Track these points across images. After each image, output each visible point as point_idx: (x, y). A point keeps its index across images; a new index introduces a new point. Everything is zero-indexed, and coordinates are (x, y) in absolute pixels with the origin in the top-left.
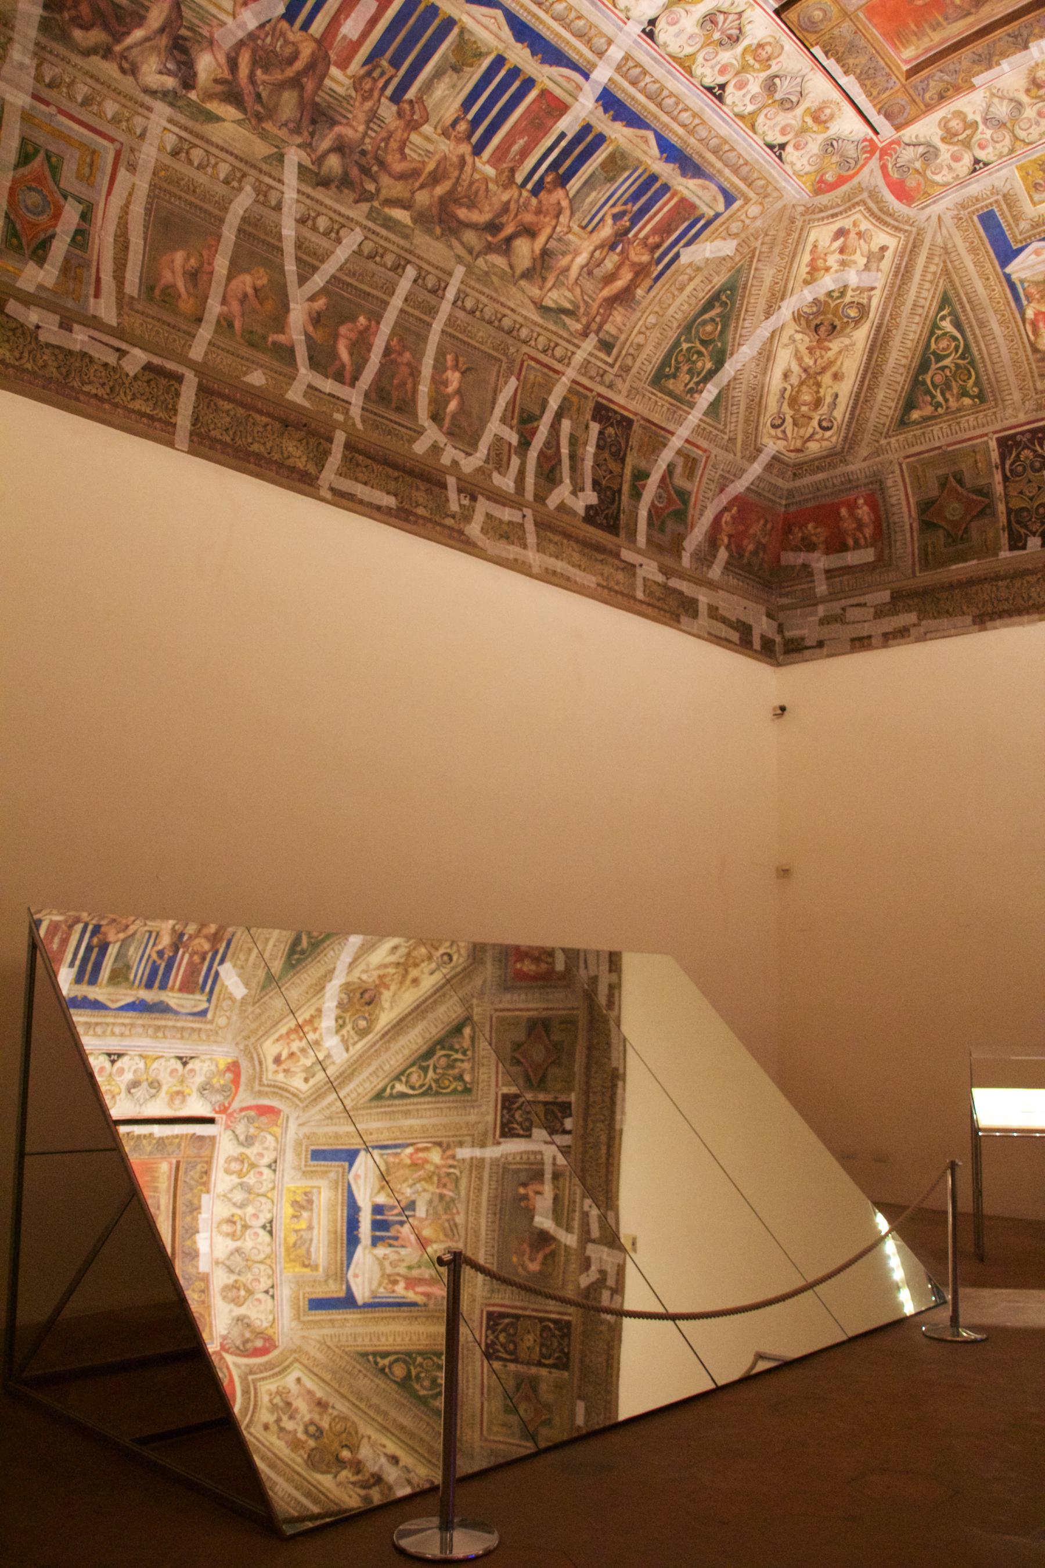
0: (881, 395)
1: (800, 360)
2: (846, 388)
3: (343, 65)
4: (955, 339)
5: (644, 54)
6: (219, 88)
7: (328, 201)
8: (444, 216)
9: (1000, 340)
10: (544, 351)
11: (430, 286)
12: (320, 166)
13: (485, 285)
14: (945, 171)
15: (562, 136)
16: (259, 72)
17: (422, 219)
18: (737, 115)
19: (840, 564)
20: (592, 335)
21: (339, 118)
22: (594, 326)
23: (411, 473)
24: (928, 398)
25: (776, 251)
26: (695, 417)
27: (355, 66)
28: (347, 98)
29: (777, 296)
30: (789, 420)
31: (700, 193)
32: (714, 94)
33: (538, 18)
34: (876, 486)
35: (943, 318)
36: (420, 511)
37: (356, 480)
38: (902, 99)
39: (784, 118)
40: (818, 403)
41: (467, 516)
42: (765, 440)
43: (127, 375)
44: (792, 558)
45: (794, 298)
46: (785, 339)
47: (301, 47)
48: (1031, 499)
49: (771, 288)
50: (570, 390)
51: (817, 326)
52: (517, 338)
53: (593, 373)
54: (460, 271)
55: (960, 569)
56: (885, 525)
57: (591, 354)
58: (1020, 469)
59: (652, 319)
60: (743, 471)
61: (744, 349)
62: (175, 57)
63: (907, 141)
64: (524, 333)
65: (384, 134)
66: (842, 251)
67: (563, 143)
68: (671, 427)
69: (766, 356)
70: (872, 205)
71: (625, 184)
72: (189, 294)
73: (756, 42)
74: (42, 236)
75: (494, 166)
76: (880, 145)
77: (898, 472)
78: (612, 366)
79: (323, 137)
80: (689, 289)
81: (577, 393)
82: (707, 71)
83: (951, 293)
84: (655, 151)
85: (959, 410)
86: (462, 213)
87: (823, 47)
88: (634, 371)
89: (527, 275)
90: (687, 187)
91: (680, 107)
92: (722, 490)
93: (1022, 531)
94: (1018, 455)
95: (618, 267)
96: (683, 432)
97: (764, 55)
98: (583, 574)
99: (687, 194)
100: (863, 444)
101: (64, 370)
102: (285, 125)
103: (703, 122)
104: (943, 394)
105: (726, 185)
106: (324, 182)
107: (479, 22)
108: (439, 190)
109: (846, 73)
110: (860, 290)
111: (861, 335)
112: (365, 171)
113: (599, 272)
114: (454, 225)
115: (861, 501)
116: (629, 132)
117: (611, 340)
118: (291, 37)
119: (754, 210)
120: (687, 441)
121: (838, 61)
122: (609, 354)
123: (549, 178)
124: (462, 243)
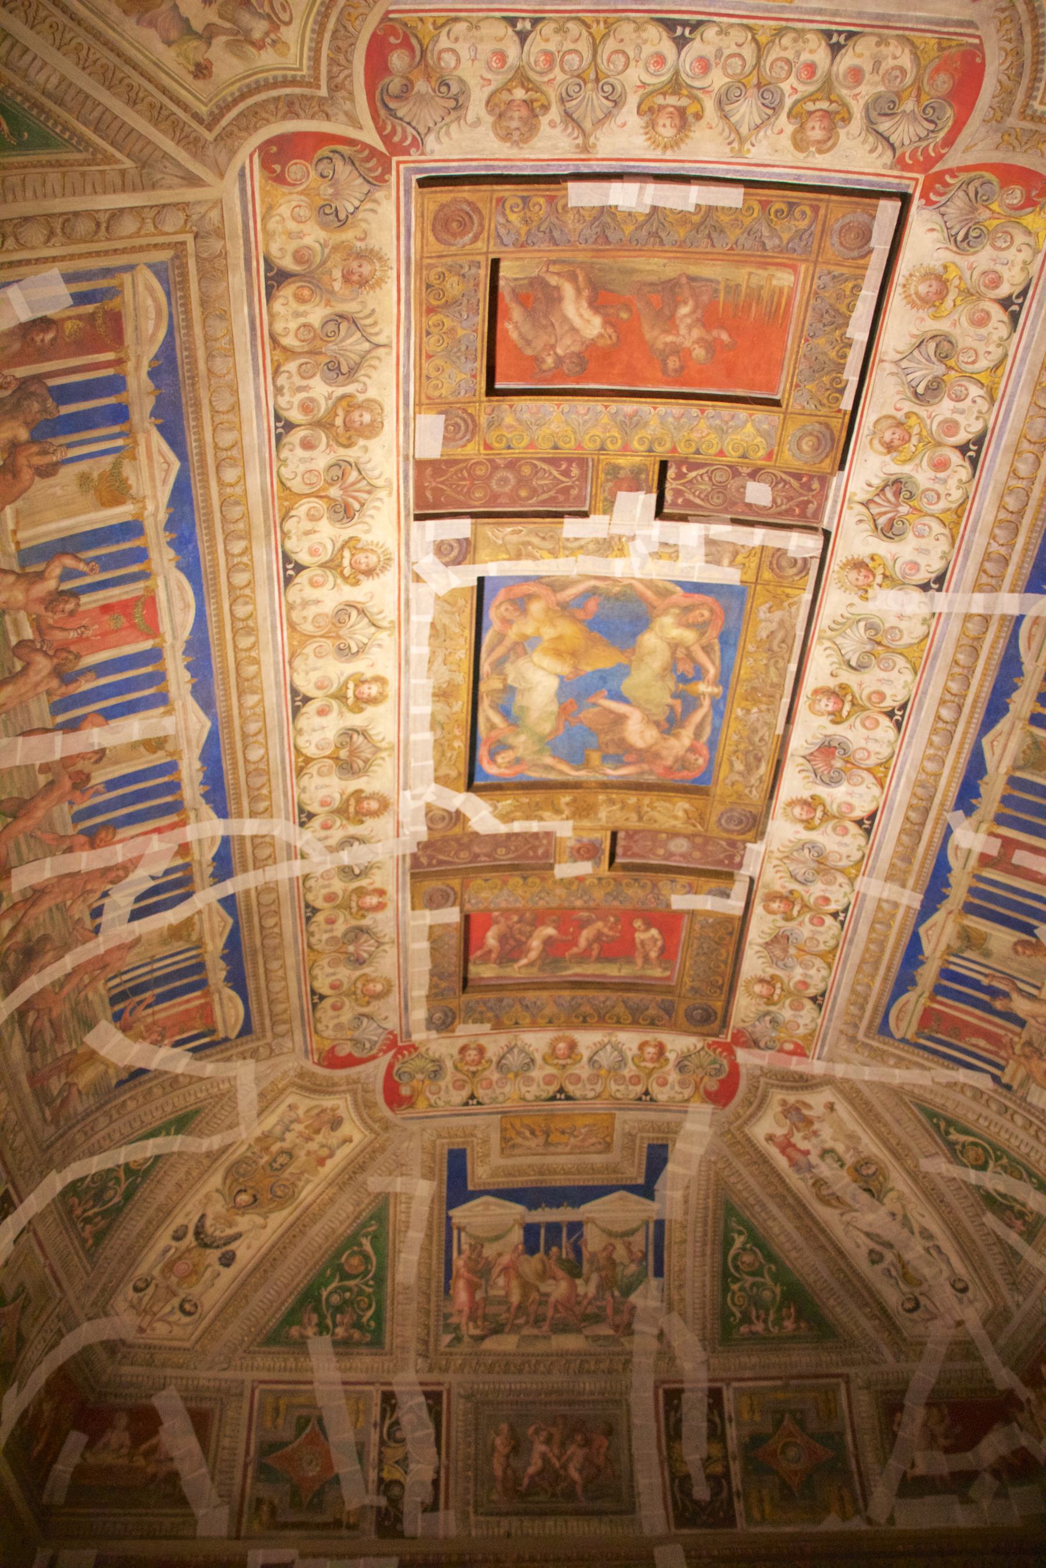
5: (967, 571)
18: (992, 401)
32: (978, 452)
33: (975, 701)
38: (833, 246)
39: (965, 335)
63: (889, 153)
73: (888, 458)
76: (921, 177)
82: (953, 483)
87: (837, 400)
91: (1013, 483)
97: (899, 433)
103: (1023, 436)
107: (1002, 755)
121: (841, 368)
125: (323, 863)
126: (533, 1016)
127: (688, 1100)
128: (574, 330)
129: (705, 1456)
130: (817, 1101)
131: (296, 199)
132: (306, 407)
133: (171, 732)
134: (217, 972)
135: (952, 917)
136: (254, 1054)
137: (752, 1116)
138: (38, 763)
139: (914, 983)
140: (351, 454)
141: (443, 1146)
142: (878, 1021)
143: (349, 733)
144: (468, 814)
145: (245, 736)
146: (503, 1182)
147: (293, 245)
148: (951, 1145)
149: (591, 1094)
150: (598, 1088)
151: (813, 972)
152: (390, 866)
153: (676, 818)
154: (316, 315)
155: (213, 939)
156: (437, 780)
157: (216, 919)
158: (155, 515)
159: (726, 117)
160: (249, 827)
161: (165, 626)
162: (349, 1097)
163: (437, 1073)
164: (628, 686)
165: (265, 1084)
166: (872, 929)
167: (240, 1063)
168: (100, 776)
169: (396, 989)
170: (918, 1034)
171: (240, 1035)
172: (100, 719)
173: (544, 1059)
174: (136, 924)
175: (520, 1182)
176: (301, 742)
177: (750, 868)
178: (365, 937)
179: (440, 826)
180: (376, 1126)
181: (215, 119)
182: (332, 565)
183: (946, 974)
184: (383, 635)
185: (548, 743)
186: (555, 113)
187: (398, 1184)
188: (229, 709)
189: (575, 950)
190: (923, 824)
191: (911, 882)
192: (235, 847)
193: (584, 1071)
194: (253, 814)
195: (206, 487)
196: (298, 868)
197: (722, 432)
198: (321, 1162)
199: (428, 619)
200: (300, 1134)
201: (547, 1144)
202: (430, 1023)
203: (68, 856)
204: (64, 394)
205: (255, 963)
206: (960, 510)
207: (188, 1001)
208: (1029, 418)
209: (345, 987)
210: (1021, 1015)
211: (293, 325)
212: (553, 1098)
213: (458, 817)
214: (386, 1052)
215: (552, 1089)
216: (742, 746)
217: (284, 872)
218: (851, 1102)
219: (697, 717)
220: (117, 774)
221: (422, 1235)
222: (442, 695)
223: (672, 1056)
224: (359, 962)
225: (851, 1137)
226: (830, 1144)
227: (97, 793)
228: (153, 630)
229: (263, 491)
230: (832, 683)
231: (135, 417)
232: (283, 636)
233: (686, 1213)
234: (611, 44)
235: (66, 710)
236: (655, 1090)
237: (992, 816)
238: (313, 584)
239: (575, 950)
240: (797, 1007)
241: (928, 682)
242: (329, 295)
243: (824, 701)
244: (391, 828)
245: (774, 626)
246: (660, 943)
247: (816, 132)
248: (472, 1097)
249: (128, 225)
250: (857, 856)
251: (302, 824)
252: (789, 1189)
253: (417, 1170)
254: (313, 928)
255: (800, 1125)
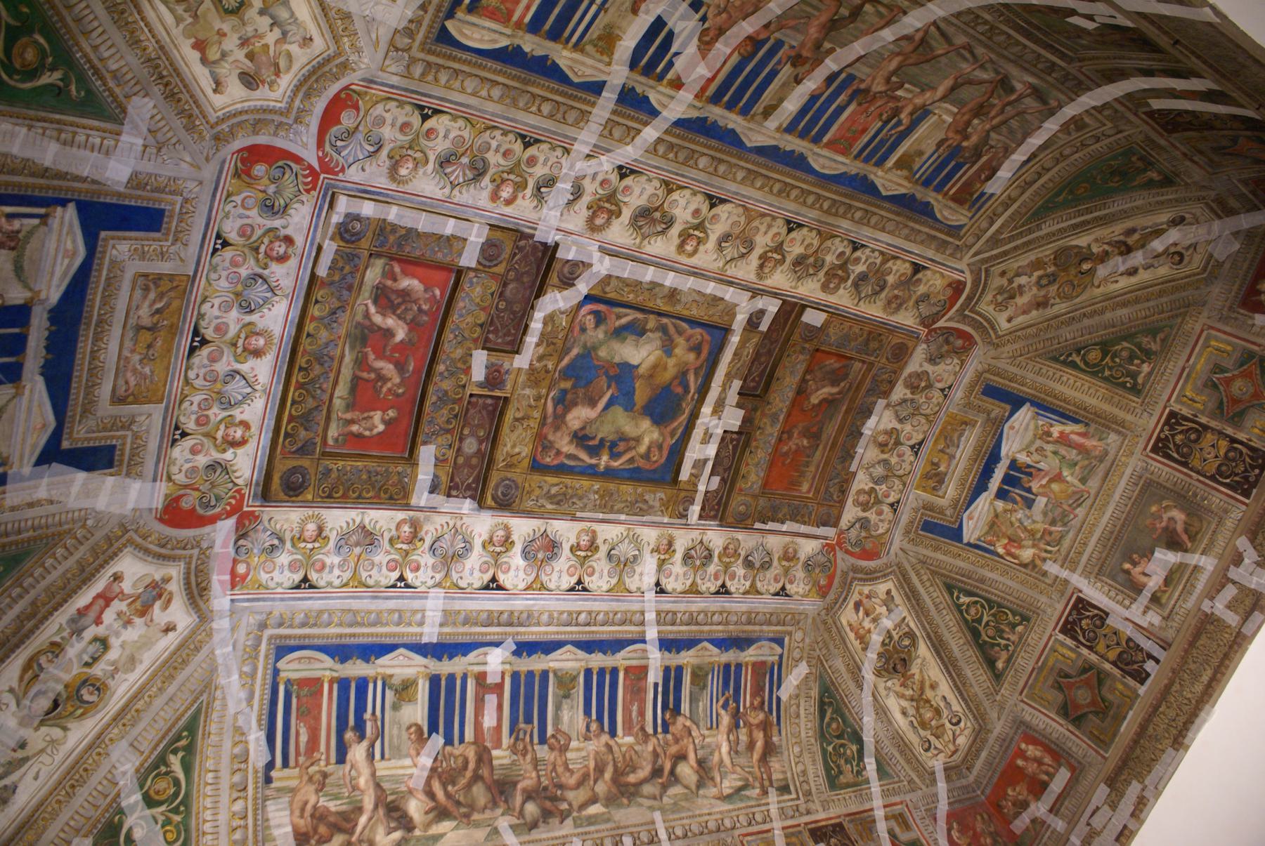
0: (969, 674)
1: (903, 696)
2: (945, 688)
3: (498, 745)
4: (976, 602)
5: (667, 604)
6: (431, 816)
7: (544, 836)
8: (623, 789)
9: (1000, 579)
10: (750, 824)
11: (646, 840)
12: (524, 817)
13: (678, 811)
14: (881, 524)
15: (656, 685)
16: (450, 788)
17: (610, 801)
19: (1053, 797)
20: (770, 789)
21: (516, 779)
22: (766, 783)
24: (997, 648)
25: (832, 647)
26: (875, 787)
27: (506, 740)
28: (514, 763)
29: (855, 672)
30: (932, 739)
31: (760, 652)
34: (1023, 728)
35: (958, 598)
38: (823, 510)
39: (770, 574)
40: (938, 712)
42: (930, 764)
44: (1021, 824)
45: (866, 664)
46: (883, 693)
47: (466, 753)
48: (1118, 644)
49: (848, 670)
50: (787, 836)
51: (894, 668)
52: (727, 830)
53: (791, 813)
54: (657, 816)
55: (1128, 727)
56: (1053, 746)
57: (779, 802)
58: (1092, 634)
59: (797, 749)
60: (936, 795)
61: (866, 719)
62: (392, 818)
64: (728, 823)
65: (550, 768)
66: (867, 614)
67: (660, 689)
68: (867, 807)
69: (882, 712)
70: (859, 576)
71: (714, 683)
75: (629, 735)
77: (1026, 707)
78: (798, 798)
79: (513, 796)
80: (802, 712)
81: (793, 834)
82: (709, 584)
83: (948, 581)
84: (715, 650)
85: (1020, 639)
86: (632, 778)
88: (814, 790)
89: (700, 785)
90: (750, 655)
92: (935, 819)
93: (1135, 667)
94: (1081, 628)
95: (750, 735)
96: (877, 802)
99: (753, 659)
100: (988, 710)
102: (485, 808)
103: (729, 613)
104: (1002, 638)
105: (771, 635)
106: (534, 826)
108: (608, 775)
109: (783, 523)
110: (897, 626)
111: (923, 650)
112: (554, 799)
113: (741, 748)
114: (632, 789)
115: (1023, 746)
116: (692, 652)
117: (783, 783)
118: (457, 752)
119: (798, 636)
120: (885, 807)
121: (773, 521)
122: (790, 793)
123: (668, 716)
124: (647, 798)
125: (572, 167)
126: (321, 318)
127: (169, 479)
128: (817, 390)
130: (179, 614)
131: (939, 287)
132: (857, 260)
133: (767, 124)
134: (531, 45)
135: (423, 669)
136: (409, 33)
137: (147, 551)
138: (838, 50)
139: (343, 660)
140: (821, 274)
141: (172, 204)
142: (292, 642)
143: (669, 222)
144: (565, 292)
145: (721, 161)
146: (101, 275)
147: (924, 280)
148: (162, 760)
149: (191, 375)
150: (199, 383)
151: (336, 572)
152: (533, 216)
153: (514, 446)
154: (891, 279)
155: (571, 59)
156: (609, 276)
157: (588, 71)
158: (875, 174)
159: (879, 462)
160: (650, 133)
161: (825, 152)
162: (283, 105)
163: (269, 208)
164: (618, 411)
165: (359, 25)
166: (391, 611)
167: (409, 14)
168: (787, 71)
169: (393, 187)
170: (289, 682)
171: (444, 30)
172: (818, 92)
173: (250, 324)
174: (651, 19)
175: (95, 297)
176: (687, 193)
177: (449, 505)
178: (470, 175)
179: (566, 270)
180: (225, 127)
181: (987, 270)
182: (779, 248)
183: (362, 684)
184: (721, 264)
185: (589, 353)
186: (909, 396)
187: (131, 140)
188: (747, 161)
189: (372, 357)
190: (499, 625)
191: (447, 630)
192: (644, 118)
193: (222, 367)
194: (659, 141)
195: (863, 202)
196: (581, 148)
197: (757, 465)
198: (200, 46)
199: (727, 297)
200: (258, 35)
201: (139, 328)
202: (352, 217)
203: (765, 22)
204: (958, 167)
205: (514, 78)
206: (699, 592)
207: (528, 8)
208: (736, 613)
209: (423, 141)
210: (349, 757)
211: (895, 268)
212: (196, 332)
213: (567, 283)
214: (320, 160)
215: (209, 333)
216: (570, 491)
217: (587, 137)
218: (181, 647)
219: (583, 456)
220: (776, 80)
221: (48, 162)
222: (673, 294)
223: (229, 455)
224: (445, 162)
225: (132, 661)
226: (115, 642)
227: (779, 62)
228: (831, 145)
229: (838, 227)
230: (599, 541)
231: (919, 188)
232: (763, 208)
233: (13, 509)
234: (923, 421)
235: (844, 81)
236: (188, 443)
237: (516, 669)
238: (778, 234)
239: (372, 357)
240: (293, 567)
241: (603, 600)
242: (895, 287)
243: (586, 538)
244: (570, 226)
245: (651, 503)
246: (367, 433)
247: (863, 498)
248: (226, 244)
249: (984, 225)
250: (462, 584)
251: (620, 168)
252: (45, 618)
253: (148, 167)
254: (511, 137)
255: (138, 605)
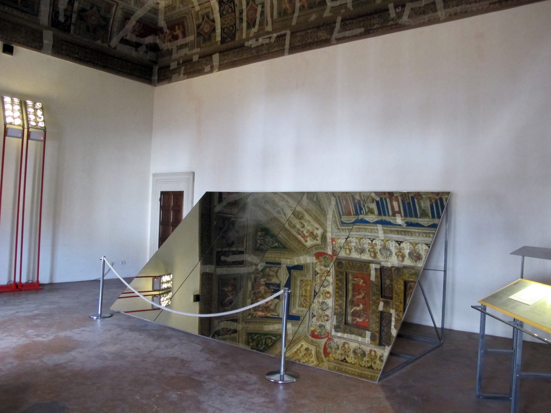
23: (371, 14)
36: (375, 27)
37: (346, 30)
41: (400, 16)
43: (272, 43)
72: (290, 7)
74: (254, 20)
98: (477, 5)
101: (257, 52)
129: (65, 8)
